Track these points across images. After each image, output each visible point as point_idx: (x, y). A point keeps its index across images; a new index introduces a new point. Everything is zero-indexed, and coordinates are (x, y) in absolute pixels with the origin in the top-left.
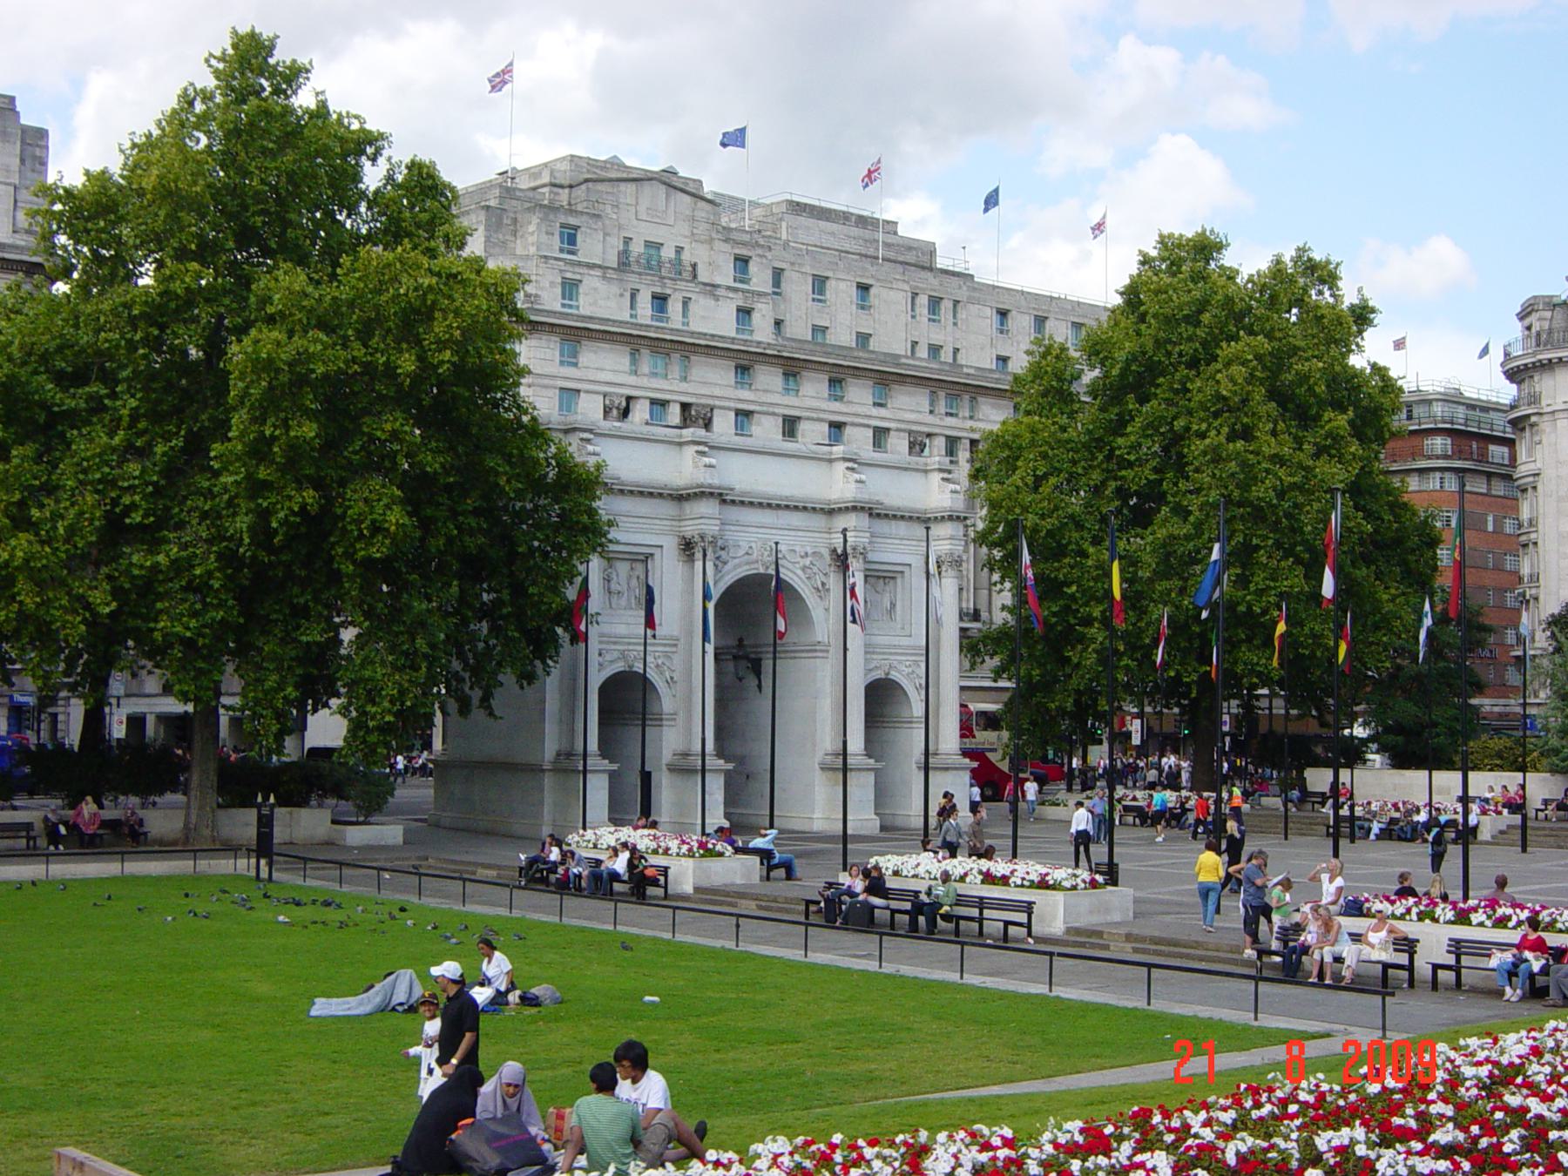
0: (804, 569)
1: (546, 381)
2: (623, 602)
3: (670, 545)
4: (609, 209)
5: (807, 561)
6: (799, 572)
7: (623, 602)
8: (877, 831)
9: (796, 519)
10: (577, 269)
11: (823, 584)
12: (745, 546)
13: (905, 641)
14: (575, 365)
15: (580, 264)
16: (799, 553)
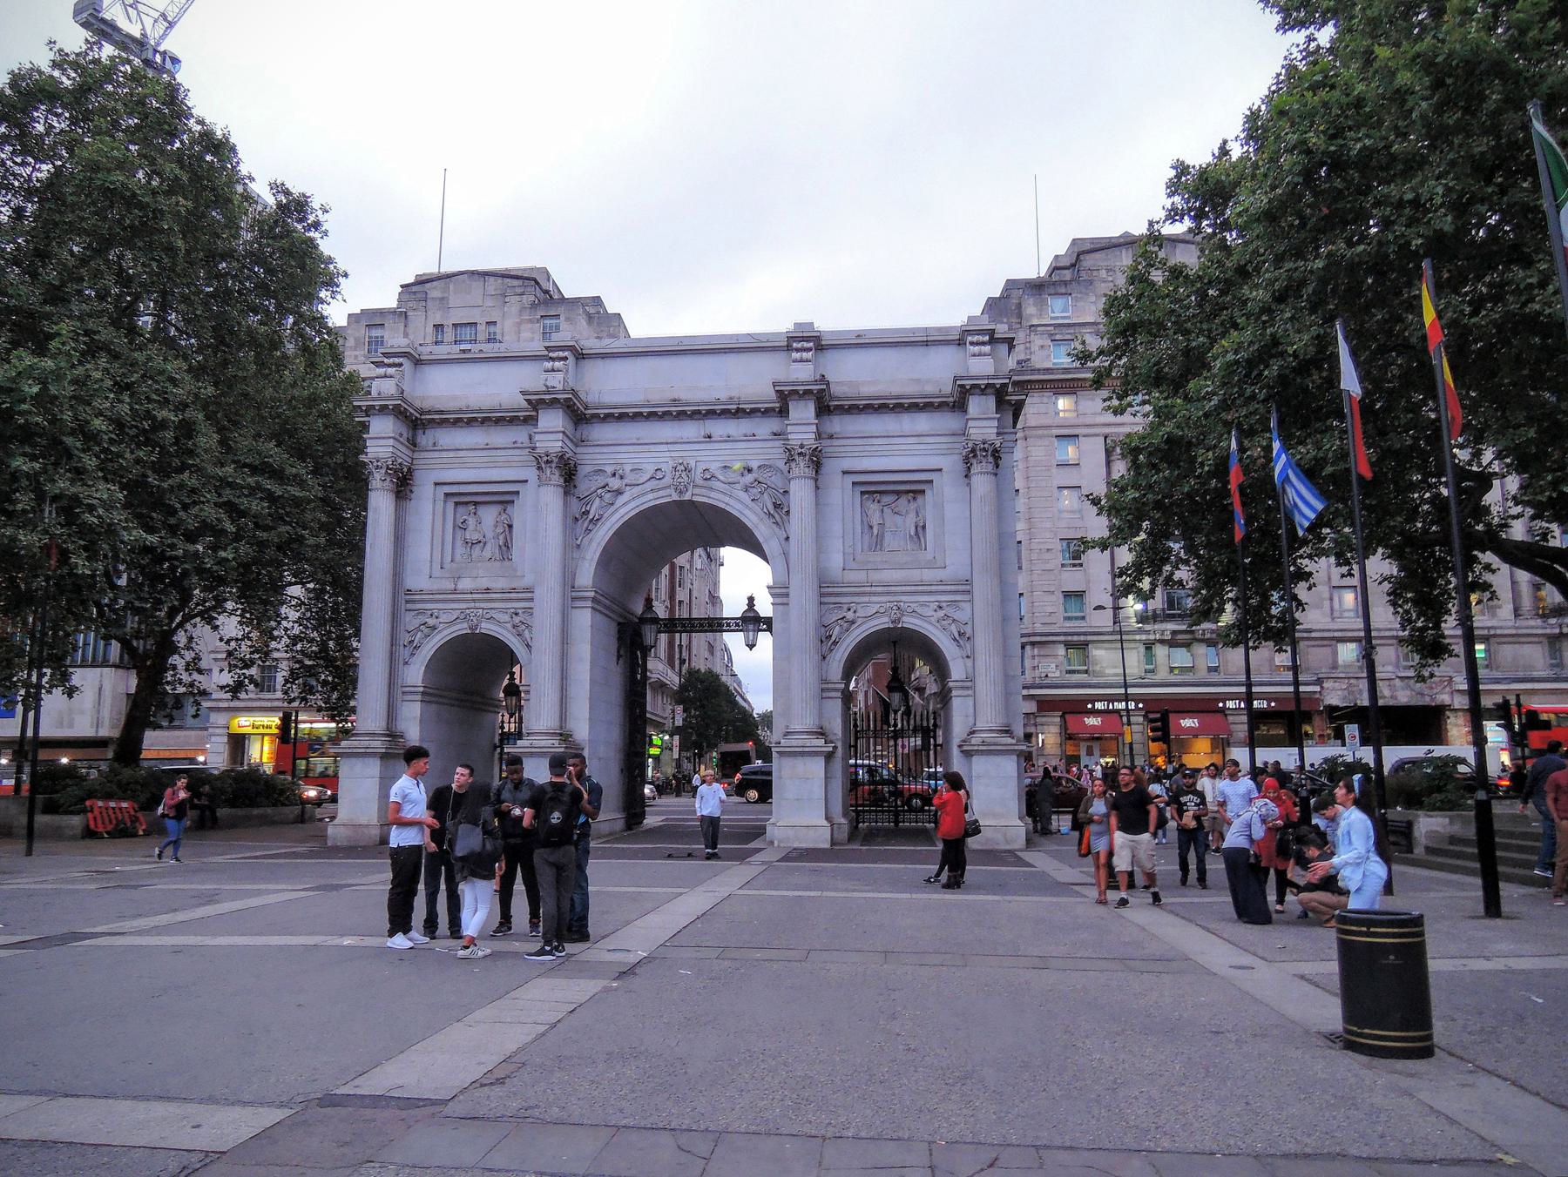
1: (1040, 432)
3: (531, 474)
4: (1103, 273)
5: (749, 478)
6: (742, 495)
7: (487, 553)
8: (827, 845)
10: (1065, 330)
11: (777, 506)
12: (650, 469)
13: (928, 575)
15: (1069, 325)
16: (721, 464)
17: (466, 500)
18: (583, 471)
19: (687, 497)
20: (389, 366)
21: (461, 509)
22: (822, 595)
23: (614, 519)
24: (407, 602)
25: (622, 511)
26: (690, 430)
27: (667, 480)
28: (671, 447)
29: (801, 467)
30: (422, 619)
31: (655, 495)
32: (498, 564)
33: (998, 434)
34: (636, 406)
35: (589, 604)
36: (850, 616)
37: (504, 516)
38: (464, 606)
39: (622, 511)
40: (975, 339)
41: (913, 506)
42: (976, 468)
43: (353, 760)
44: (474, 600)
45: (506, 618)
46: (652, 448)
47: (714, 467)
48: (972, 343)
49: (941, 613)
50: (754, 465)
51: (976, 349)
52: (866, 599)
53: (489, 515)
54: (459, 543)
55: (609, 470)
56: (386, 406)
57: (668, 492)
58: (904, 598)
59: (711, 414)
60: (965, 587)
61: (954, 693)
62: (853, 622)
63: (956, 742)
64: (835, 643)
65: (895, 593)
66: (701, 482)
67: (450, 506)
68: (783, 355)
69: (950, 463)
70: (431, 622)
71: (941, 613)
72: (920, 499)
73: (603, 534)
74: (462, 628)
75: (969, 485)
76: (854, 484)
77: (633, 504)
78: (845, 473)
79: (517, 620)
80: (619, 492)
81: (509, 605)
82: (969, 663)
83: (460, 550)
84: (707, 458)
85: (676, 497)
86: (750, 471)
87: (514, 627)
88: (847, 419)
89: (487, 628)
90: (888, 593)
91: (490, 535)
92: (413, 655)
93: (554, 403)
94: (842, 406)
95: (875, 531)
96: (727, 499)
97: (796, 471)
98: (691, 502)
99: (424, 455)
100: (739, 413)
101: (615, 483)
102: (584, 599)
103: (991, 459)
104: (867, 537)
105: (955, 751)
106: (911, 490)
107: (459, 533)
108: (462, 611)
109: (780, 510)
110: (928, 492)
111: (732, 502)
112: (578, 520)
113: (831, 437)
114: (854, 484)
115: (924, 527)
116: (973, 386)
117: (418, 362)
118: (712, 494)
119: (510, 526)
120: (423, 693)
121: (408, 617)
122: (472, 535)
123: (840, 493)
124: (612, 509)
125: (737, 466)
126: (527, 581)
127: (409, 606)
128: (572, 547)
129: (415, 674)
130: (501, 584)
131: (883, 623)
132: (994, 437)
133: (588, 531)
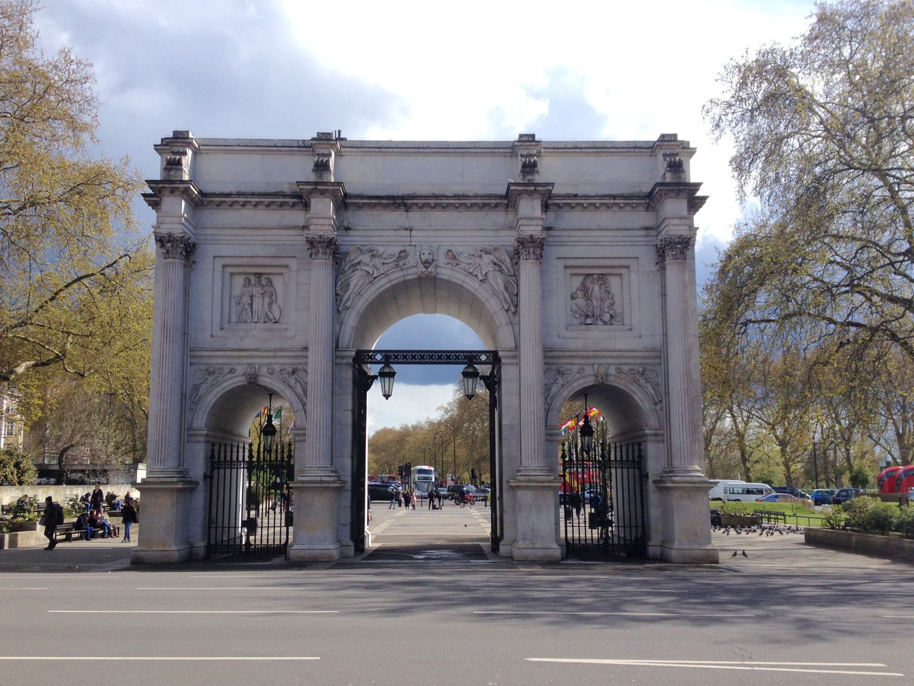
22: (545, 357)
24: (193, 357)
63: (651, 478)
75: (663, 269)
76: (566, 267)
120: (207, 435)
126: (299, 342)
127: (193, 361)
131: (590, 381)
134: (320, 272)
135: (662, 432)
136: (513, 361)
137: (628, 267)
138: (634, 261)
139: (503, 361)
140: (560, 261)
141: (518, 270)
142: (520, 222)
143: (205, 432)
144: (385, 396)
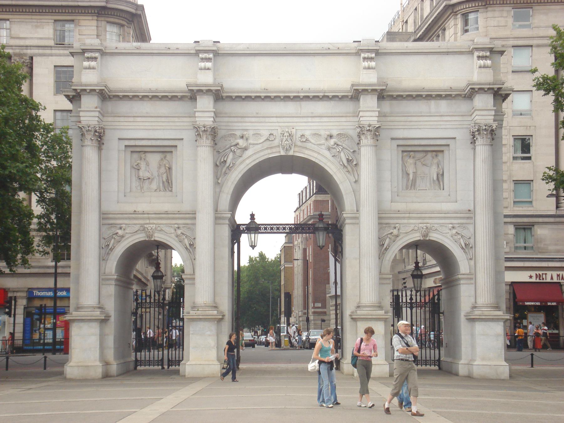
0: (329, 149)
2: (154, 186)
3: (188, 135)
5: (332, 142)
6: (327, 153)
7: (154, 186)
9: (321, 107)
11: (349, 161)
12: (266, 134)
13: (446, 207)
14: (528, 26)
17: (138, 150)
18: (221, 133)
19: (291, 153)
20: (88, 59)
21: (135, 156)
22: (380, 218)
23: (242, 166)
24: (104, 219)
25: (248, 161)
26: (290, 108)
27: (276, 142)
28: (279, 120)
29: (367, 140)
30: (114, 230)
31: (269, 151)
32: (162, 193)
33: (494, 120)
34: (257, 92)
35: (227, 222)
36: (395, 232)
37: (165, 162)
38: (141, 222)
39: (248, 161)
40: (481, 54)
41: (435, 161)
42: (480, 141)
43: (82, 324)
44: (149, 218)
45: (173, 231)
46: (267, 120)
47: (307, 133)
48: (479, 57)
49: (454, 231)
50: (335, 133)
51: (482, 62)
52: (405, 221)
53: (154, 159)
54: (134, 179)
55: (238, 133)
56: (94, 90)
57: (277, 149)
58: (430, 221)
59: (307, 98)
60: (470, 214)
61: (462, 282)
62: (397, 236)
63: (463, 314)
64: (386, 249)
65: (425, 218)
66: (299, 144)
67: (129, 154)
68: (353, 58)
69: (462, 136)
70: (120, 232)
71: (454, 231)
72: (440, 155)
73: (235, 176)
74: (141, 237)
75: (475, 149)
77: (254, 157)
78: (392, 139)
79: (179, 232)
80: (245, 149)
81: (174, 222)
82: (472, 262)
83: (135, 183)
84: (305, 128)
85: (283, 153)
86: (331, 137)
87: (177, 236)
88: (395, 102)
89: (158, 237)
90: (419, 218)
91: (156, 174)
92: (108, 254)
93: (209, 91)
94: (392, 96)
95: (411, 177)
96: (316, 155)
97: (364, 141)
98: (293, 156)
99: (110, 119)
100: (325, 98)
101: (242, 143)
102: (224, 218)
103: (489, 136)
104: (405, 180)
105: (463, 319)
106: (435, 151)
107: (133, 171)
108: (142, 225)
109: (352, 165)
110: (446, 153)
111: (319, 157)
112: (220, 167)
113: (385, 116)
114: (398, 146)
115: (443, 175)
116: (480, 89)
117: (103, 53)
118: (307, 152)
119: (170, 169)
120: (116, 280)
121: (104, 228)
122: (143, 173)
123: (391, 154)
124: (241, 159)
125: (324, 133)
126: (186, 207)
128: (218, 183)
129: (112, 266)
130: (167, 207)
132: (491, 122)
133: (225, 173)
134: (205, 153)
135: (471, 276)
136: (354, 221)
137: (448, 145)
138: (453, 140)
139: (347, 221)
140: (394, 141)
141: (359, 149)
142: (361, 114)
143: (116, 277)
144: (251, 246)
